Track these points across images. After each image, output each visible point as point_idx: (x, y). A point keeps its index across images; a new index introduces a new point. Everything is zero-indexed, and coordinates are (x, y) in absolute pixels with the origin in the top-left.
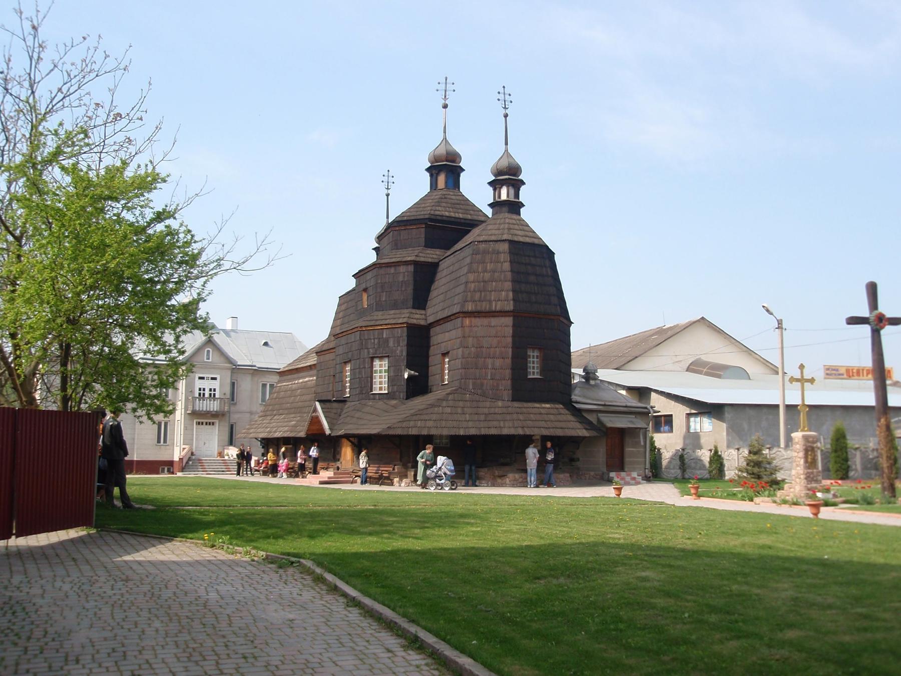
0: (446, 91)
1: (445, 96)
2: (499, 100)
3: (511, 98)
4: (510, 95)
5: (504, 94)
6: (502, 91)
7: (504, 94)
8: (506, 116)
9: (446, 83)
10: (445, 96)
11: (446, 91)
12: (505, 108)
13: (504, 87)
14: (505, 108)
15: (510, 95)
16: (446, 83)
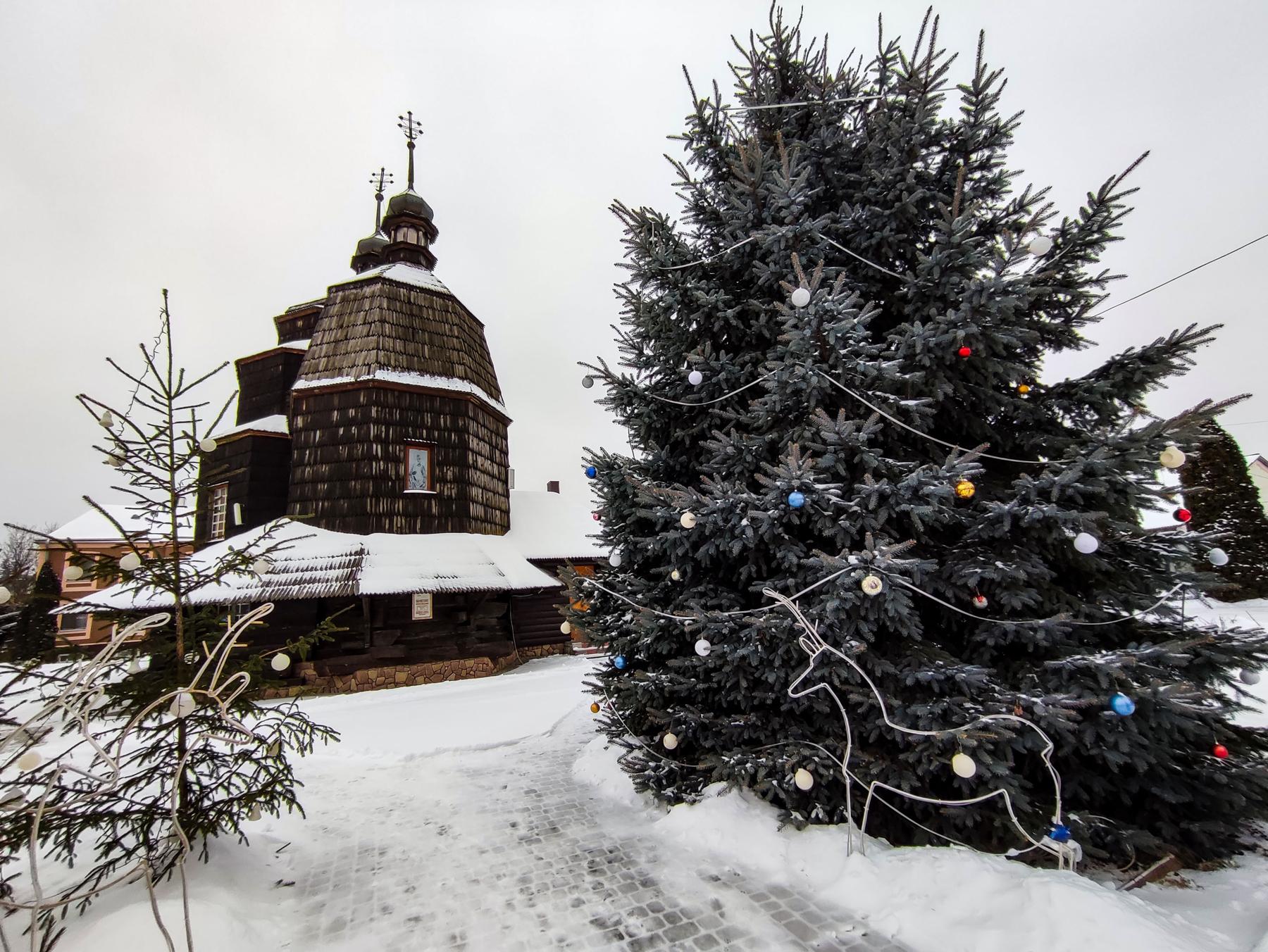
0: (381, 182)
1: (381, 187)
2: (400, 125)
3: (421, 128)
4: (419, 124)
5: (410, 120)
6: (406, 116)
7: (410, 120)
8: (411, 146)
9: (382, 175)
10: (381, 187)
11: (381, 182)
12: (411, 137)
13: (410, 113)
14: (411, 137)
15: (419, 124)
16: (382, 175)
